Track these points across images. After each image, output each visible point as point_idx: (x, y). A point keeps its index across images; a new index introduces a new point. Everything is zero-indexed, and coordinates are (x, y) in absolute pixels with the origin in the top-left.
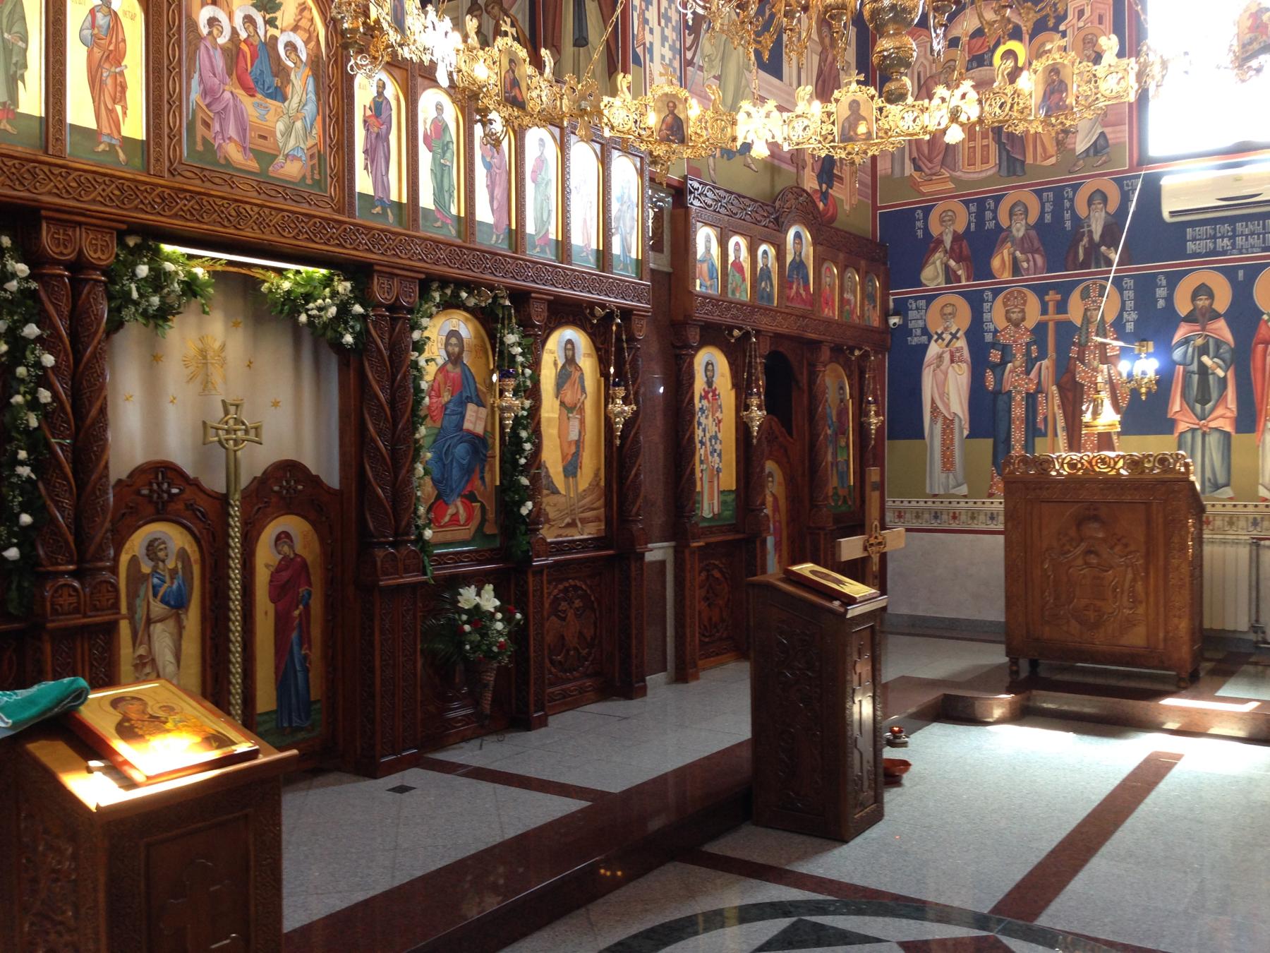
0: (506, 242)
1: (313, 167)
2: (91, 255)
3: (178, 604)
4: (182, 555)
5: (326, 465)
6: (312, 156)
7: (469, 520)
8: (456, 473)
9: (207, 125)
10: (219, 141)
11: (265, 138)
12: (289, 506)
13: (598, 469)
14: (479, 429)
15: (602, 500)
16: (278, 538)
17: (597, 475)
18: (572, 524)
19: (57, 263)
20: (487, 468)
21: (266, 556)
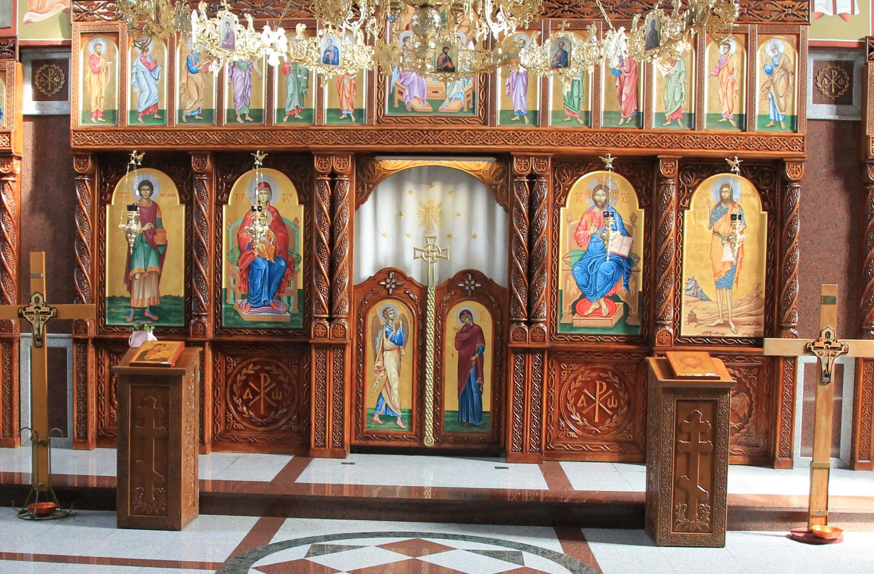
0: (634, 122)
2: (337, 169)
3: (399, 343)
5: (499, 275)
6: (468, 96)
7: (609, 315)
8: (600, 281)
10: (408, 99)
11: (437, 92)
12: (465, 295)
13: (759, 285)
14: (625, 252)
15: (763, 309)
16: (462, 314)
17: (758, 288)
18: (726, 324)
19: (323, 174)
20: (631, 279)
21: (453, 324)
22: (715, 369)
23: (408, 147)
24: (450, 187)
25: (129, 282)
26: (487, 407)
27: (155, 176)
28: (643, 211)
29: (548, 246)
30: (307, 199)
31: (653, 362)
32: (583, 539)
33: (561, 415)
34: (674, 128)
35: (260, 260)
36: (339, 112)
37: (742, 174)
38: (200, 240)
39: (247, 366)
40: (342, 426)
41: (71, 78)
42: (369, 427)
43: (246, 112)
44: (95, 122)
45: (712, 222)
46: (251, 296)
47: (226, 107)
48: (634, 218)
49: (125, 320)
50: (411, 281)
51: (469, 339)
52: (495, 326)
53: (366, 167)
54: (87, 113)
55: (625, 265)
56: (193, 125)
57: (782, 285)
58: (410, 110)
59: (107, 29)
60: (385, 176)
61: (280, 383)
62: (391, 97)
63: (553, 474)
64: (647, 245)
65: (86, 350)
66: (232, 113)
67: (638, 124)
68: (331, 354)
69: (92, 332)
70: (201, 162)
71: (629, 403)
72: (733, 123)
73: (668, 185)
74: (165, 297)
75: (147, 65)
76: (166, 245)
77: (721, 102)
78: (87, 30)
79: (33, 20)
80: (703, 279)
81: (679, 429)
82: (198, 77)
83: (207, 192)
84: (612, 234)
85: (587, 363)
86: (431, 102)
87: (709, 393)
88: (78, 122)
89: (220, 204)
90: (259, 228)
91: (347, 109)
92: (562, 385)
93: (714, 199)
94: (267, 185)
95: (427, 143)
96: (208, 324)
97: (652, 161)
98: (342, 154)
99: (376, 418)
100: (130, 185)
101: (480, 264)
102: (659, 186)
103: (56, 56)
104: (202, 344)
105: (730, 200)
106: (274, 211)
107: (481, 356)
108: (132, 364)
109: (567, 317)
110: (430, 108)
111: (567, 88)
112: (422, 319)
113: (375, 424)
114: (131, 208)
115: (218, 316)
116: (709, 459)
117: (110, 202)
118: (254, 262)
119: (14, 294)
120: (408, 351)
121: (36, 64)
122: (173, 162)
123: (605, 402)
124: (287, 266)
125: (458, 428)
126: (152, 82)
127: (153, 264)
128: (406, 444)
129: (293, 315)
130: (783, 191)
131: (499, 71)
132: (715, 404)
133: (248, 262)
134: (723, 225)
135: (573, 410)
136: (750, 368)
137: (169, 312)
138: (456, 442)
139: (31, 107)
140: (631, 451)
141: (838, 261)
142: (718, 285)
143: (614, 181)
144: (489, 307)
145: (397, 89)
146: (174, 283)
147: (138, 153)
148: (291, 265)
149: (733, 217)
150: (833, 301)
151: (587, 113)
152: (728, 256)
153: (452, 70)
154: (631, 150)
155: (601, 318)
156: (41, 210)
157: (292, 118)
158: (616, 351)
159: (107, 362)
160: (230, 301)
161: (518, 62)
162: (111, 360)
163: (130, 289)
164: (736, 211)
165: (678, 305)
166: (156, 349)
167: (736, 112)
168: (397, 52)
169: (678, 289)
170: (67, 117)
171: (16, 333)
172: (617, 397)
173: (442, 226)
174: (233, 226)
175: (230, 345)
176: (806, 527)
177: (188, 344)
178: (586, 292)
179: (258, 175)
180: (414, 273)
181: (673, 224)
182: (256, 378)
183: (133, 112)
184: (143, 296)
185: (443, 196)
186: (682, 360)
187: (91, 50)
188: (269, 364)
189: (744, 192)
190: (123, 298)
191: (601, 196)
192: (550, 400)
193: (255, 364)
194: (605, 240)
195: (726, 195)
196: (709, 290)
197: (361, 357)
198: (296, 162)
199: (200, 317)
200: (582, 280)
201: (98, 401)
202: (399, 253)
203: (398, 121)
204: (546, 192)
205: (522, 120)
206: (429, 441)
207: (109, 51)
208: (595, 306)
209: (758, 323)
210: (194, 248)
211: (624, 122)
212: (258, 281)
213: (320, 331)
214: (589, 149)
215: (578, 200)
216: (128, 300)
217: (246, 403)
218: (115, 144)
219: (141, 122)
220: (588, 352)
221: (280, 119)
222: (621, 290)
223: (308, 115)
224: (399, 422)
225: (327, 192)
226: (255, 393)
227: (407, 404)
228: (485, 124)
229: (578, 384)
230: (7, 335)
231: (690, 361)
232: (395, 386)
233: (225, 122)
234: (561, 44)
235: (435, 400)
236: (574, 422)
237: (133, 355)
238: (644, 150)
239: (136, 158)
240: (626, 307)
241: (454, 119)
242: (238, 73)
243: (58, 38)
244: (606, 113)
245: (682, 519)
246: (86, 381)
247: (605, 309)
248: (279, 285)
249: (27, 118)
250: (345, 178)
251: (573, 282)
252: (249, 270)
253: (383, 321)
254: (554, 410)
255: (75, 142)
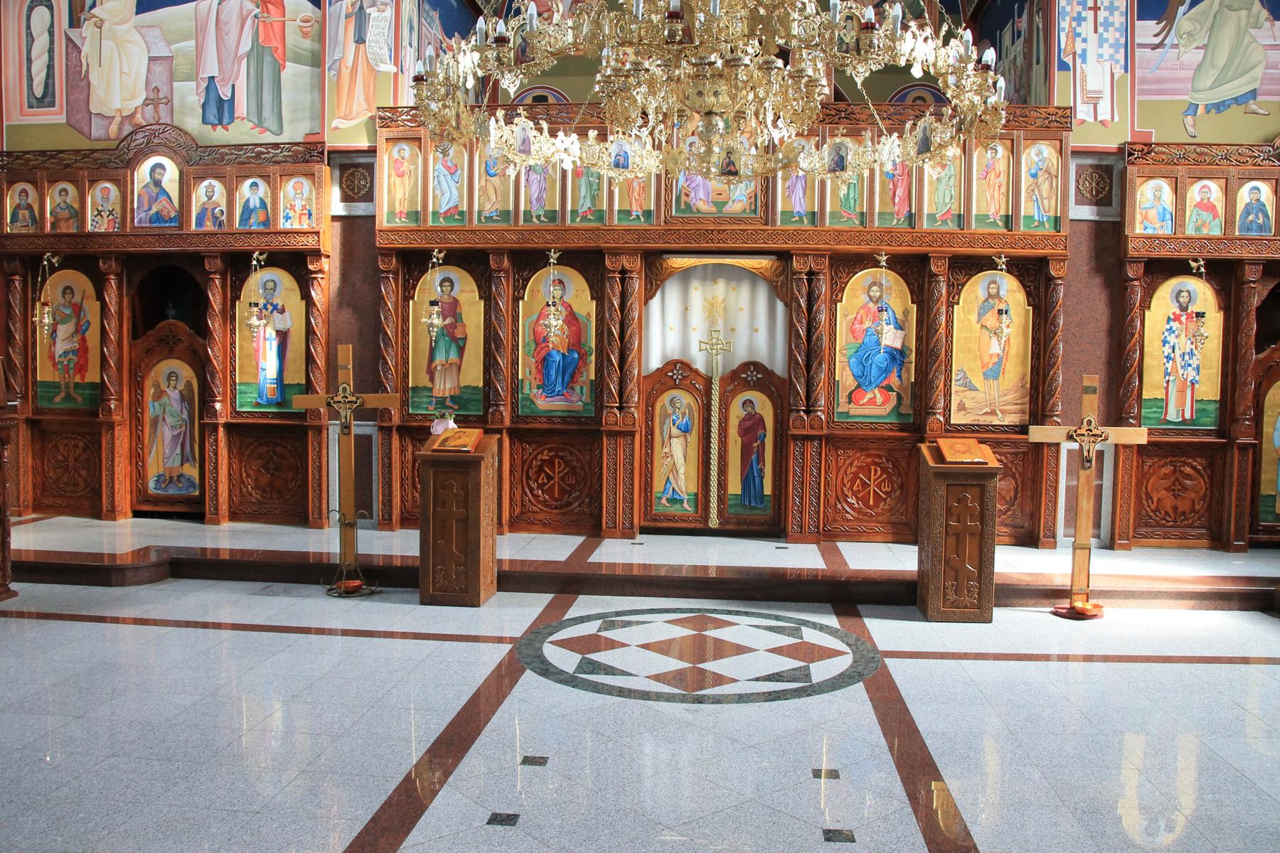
2: (627, 266)
3: (686, 431)
4: (689, 406)
5: (779, 366)
7: (883, 404)
8: (874, 372)
12: (748, 385)
14: (898, 345)
18: (993, 413)
19: (614, 272)
22: (984, 455)
23: (694, 245)
24: (733, 284)
25: (431, 373)
26: (768, 490)
27: (456, 273)
28: (915, 307)
29: (825, 339)
30: (598, 294)
31: (924, 448)
32: (858, 615)
33: (837, 498)
34: (944, 228)
35: (554, 352)
36: (629, 213)
37: (1008, 271)
38: (497, 333)
39: (542, 452)
40: (632, 509)
41: (377, 181)
42: (657, 509)
43: (542, 213)
44: (399, 223)
45: (980, 316)
46: (546, 386)
47: (522, 208)
48: (906, 313)
49: (427, 409)
50: (696, 371)
51: (751, 426)
52: (776, 415)
53: (654, 265)
54: (392, 214)
55: (898, 357)
56: (491, 225)
57: (1046, 375)
59: (411, 134)
60: (672, 273)
61: (573, 468)
62: (678, 198)
63: (831, 554)
64: (919, 338)
65: (390, 437)
66: (528, 214)
67: (910, 224)
68: (621, 441)
69: (396, 420)
70: (499, 259)
71: (902, 487)
72: (1000, 224)
73: (938, 282)
74: (465, 387)
75: (448, 168)
76: (465, 339)
77: (988, 203)
78: (392, 135)
79: (341, 126)
80: (971, 370)
81: (949, 511)
82: (496, 180)
83: (504, 289)
84: (886, 328)
85: (862, 450)
86: (716, 204)
87: (978, 477)
88: (383, 222)
89: (517, 299)
90: (554, 323)
91: (636, 210)
92: (839, 470)
93: (982, 294)
94: (561, 282)
95: (712, 242)
96: (506, 412)
97: (923, 259)
98: (631, 252)
99: (664, 501)
100: (432, 282)
101: (762, 356)
102: (930, 283)
103: (362, 160)
104: (499, 431)
105: (997, 296)
106: (568, 307)
107: (763, 443)
108: (434, 451)
109: (843, 408)
110: (714, 210)
111: (843, 190)
112: (707, 408)
113: (662, 506)
114: (433, 303)
115: (514, 406)
116: (977, 538)
117: (413, 298)
118: (549, 354)
119: (323, 384)
120: (693, 438)
121: (343, 168)
122: (472, 260)
123: (879, 486)
124: (580, 358)
125: (741, 511)
126: (452, 184)
127: (453, 356)
128: (692, 525)
129: (585, 404)
130: (1047, 287)
131: (780, 174)
132: (983, 488)
133: (543, 354)
134: (991, 319)
135: (849, 494)
136: (1016, 454)
137: (469, 401)
138: (739, 523)
139: (339, 209)
140: (903, 533)
141: (1099, 353)
142: (986, 376)
143: (888, 277)
144: (770, 397)
146: (473, 374)
147: (440, 252)
148: (583, 357)
149: (1000, 312)
150: (1094, 391)
151: (862, 214)
152: (995, 348)
153: (736, 173)
154: (904, 249)
155: (875, 408)
156: (349, 305)
158: (889, 438)
159: (410, 449)
160: (526, 391)
161: (797, 166)
162: (414, 446)
163: (432, 380)
164: (1002, 306)
165: (948, 394)
166: (456, 436)
167: (1003, 213)
168: (683, 156)
169: (948, 380)
170: (373, 217)
171: (325, 421)
172: (891, 481)
173: (726, 320)
174: (529, 320)
175: (526, 432)
176: (1068, 603)
177: (486, 432)
178: (862, 382)
179: (552, 272)
180: (700, 365)
181: (943, 318)
182: (551, 463)
183: (434, 213)
184: (444, 386)
185: (727, 292)
186: (951, 447)
187: (395, 155)
188: (563, 450)
189: (1010, 288)
190: (425, 388)
191: (875, 292)
192: (827, 484)
193: (550, 450)
194: (879, 333)
195: (993, 291)
196: (977, 381)
197: (649, 444)
198: (588, 261)
199: (498, 406)
200: (858, 371)
201: (402, 485)
202: (685, 345)
203: (684, 221)
204: (824, 288)
205: (801, 218)
206: (714, 522)
207: (412, 155)
208: (870, 395)
209: (1023, 412)
210: (492, 340)
211: (898, 223)
212: (553, 372)
213: (611, 419)
214: (864, 248)
215: (854, 296)
216: (431, 390)
217: (541, 486)
218: (418, 243)
219: (442, 223)
220: (864, 439)
221: (573, 220)
222: (894, 380)
224: (686, 505)
225: (618, 288)
226: (549, 478)
227: (693, 488)
228: (766, 224)
229: (854, 469)
230: (316, 423)
231: (962, 448)
232: (682, 471)
233: (521, 222)
234: (838, 148)
235: (719, 484)
236: (850, 505)
237: (435, 442)
238: (917, 249)
239: (437, 256)
240: (899, 396)
241: (737, 220)
242: (533, 176)
243: (364, 144)
244: (880, 214)
245: (952, 596)
246: (390, 466)
247: (879, 399)
248: (573, 376)
249: (335, 218)
250: (635, 275)
251: (849, 373)
252: (544, 362)
253: (670, 410)
254: (832, 493)
255: (380, 242)
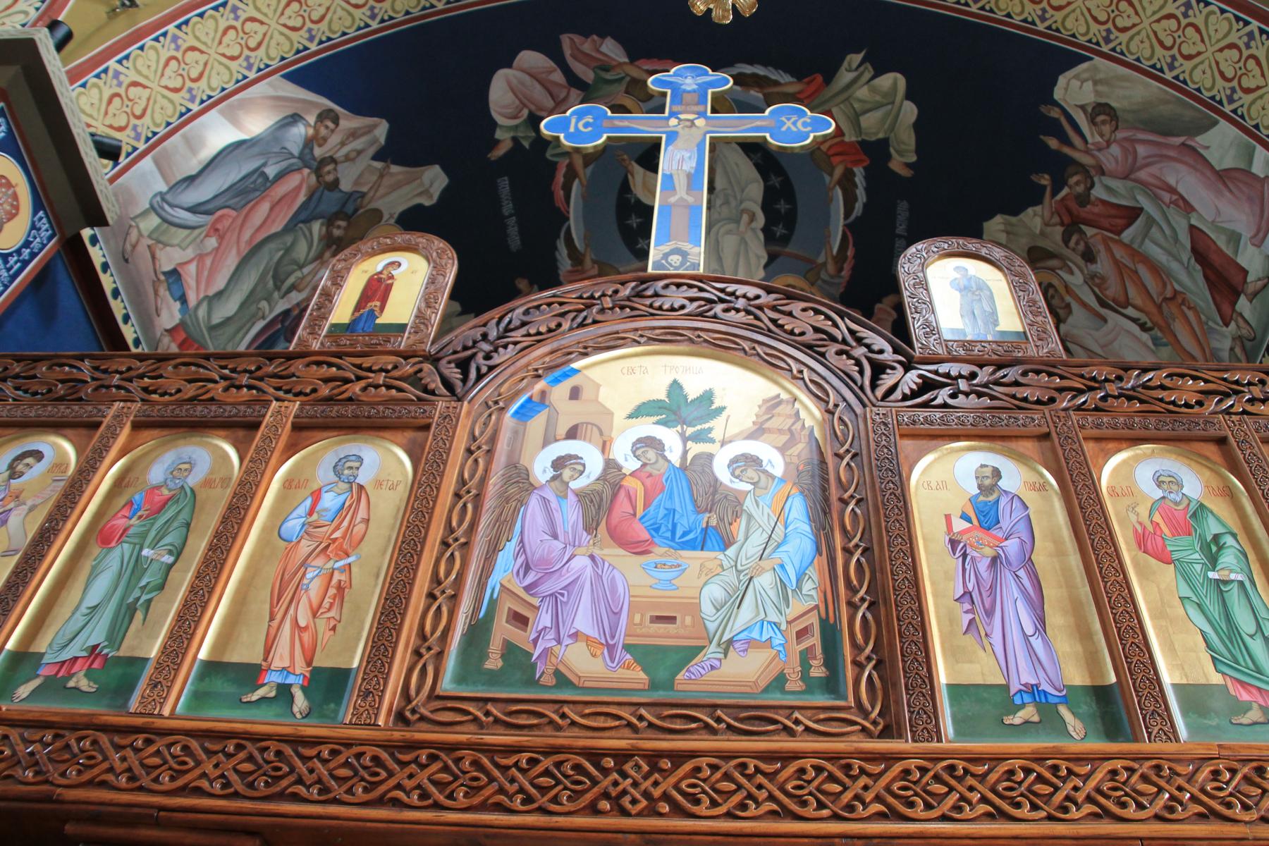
1: (806, 656)
9: (520, 620)
10: (547, 642)
11: (671, 619)
36: (250, 674)
58: (548, 680)
62: (478, 632)
91: (287, 665)
110: (638, 676)
145: (508, 604)
157: (56, 685)
205: (1049, 719)
223: (120, 673)
228: (886, 733)
241: (752, 716)
